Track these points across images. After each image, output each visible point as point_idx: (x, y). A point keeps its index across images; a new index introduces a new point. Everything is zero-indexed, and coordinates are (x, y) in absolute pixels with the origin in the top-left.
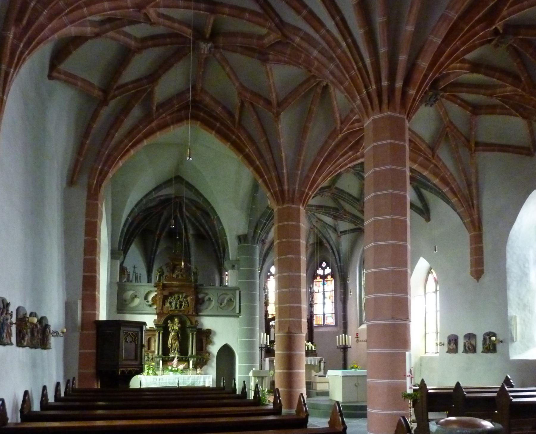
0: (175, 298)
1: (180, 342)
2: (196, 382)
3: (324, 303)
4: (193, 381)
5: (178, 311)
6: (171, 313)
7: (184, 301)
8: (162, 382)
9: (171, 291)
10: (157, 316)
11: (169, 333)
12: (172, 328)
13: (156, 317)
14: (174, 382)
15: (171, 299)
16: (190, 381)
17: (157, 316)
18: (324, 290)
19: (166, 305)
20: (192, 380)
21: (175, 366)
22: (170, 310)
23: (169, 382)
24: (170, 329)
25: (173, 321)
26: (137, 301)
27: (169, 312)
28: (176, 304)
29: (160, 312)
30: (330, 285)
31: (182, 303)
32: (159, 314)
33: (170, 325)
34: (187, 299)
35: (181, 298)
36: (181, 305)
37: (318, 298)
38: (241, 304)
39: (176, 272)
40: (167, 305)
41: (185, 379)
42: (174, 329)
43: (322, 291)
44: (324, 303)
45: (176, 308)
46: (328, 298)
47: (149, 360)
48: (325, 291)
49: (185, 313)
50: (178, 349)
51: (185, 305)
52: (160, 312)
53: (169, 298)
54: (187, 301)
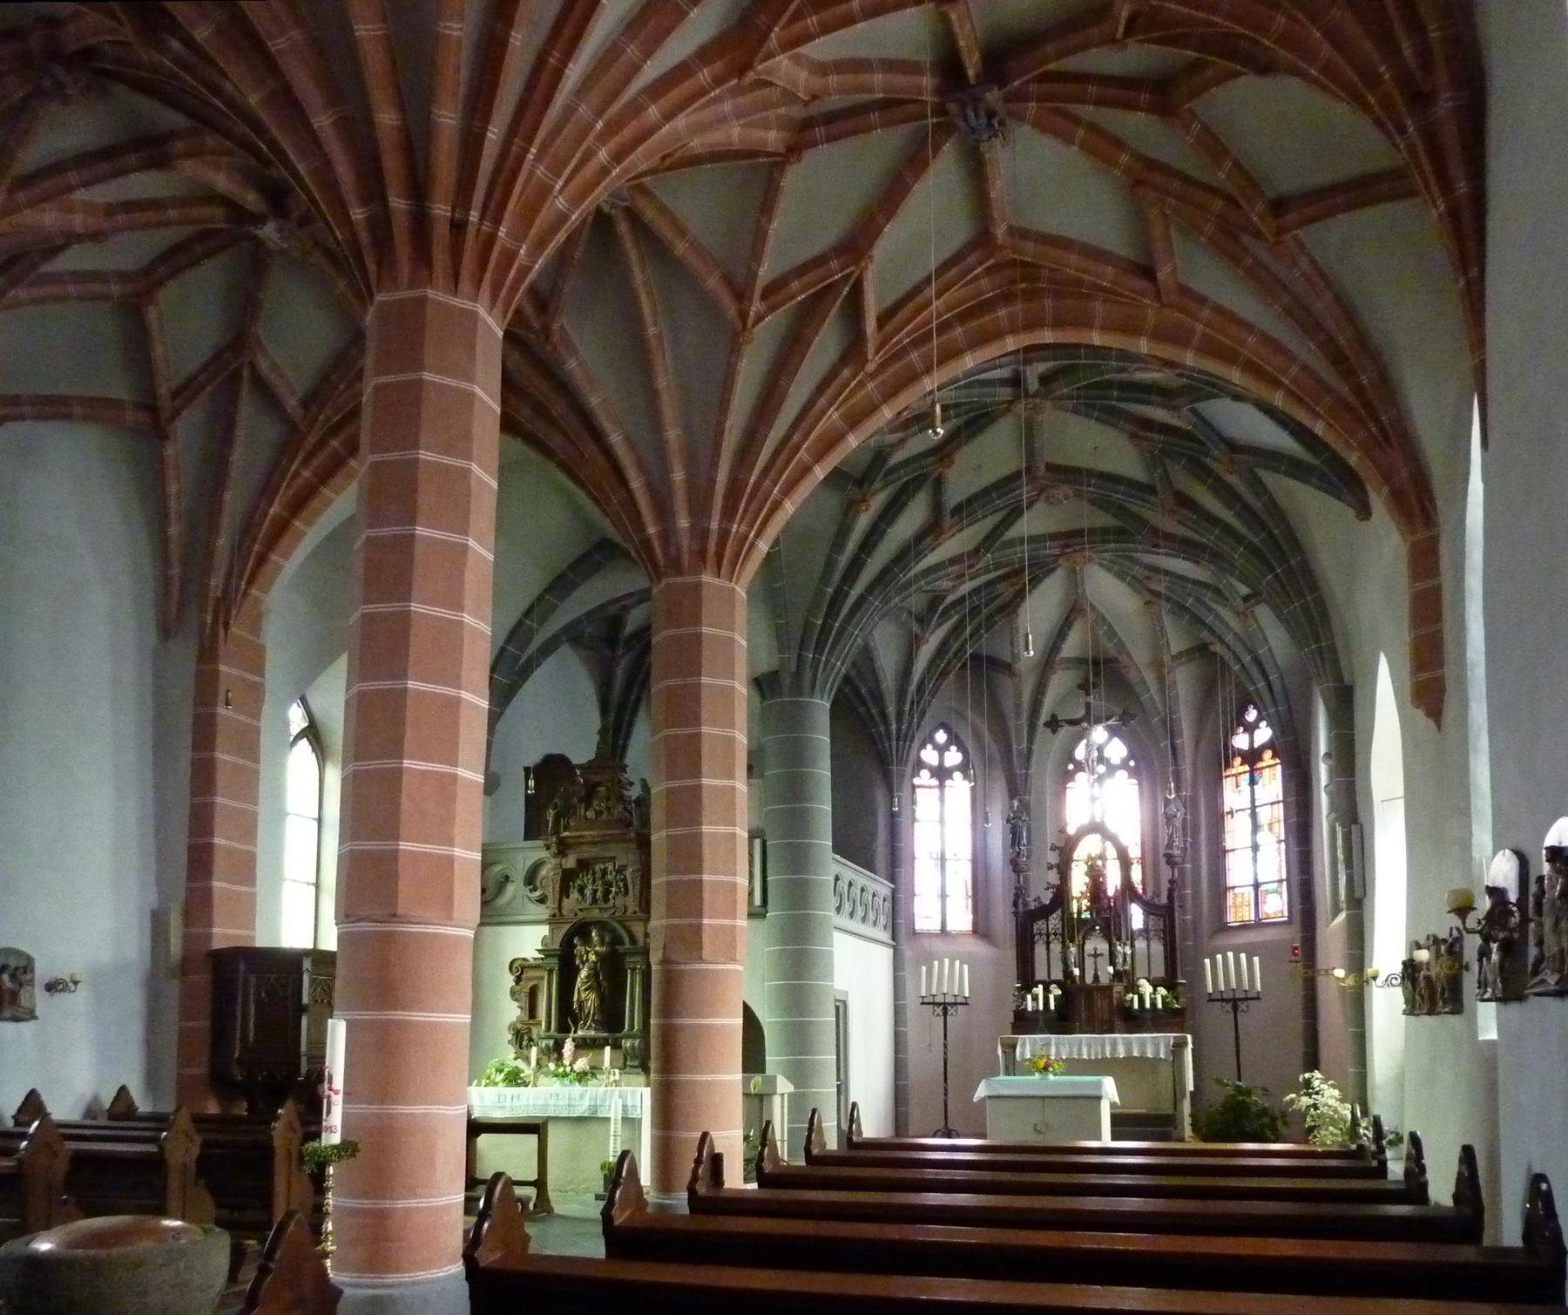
0: (594, 873)
1: (602, 998)
2: (601, 1106)
3: (1255, 848)
4: (593, 1103)
5: (600, 909)
6: (581, 915)
8: (519, 1104)
9: (586, 855)
10: (547, 927)
11: (577, 971)
12: (581, 957)
13: (544, 930)
14: (548, 1105)
16: (586, 1103)
17: (547, 927)
18: (1253, 800)
19: (571, 896)
20: (590, 1099)
21: (566, 1062)
22: (580, 910)
23: (534, 1105)
24: (577, 962)
25: (587, 940)
26: (510, 889)
28: (595, 891)
30: (1272, 783)
32: (554, 921)
33: (580, 949)
34: (625, 876)
36: (607, 893)
37: (1236, 832)
38: (769, 879)
39: (595, 802)
40: (575, 895)
41: (573, 1097)
42: (587, 960)
43: (1249, 805)
44: (1255, 848)
45: (595, 901)
46: (1266, 827)
48: (1257, 803)
49: (617, 914)
50: (594, 1015)
51: (616, 893)
52: (554, 916)
54: (625, 880)
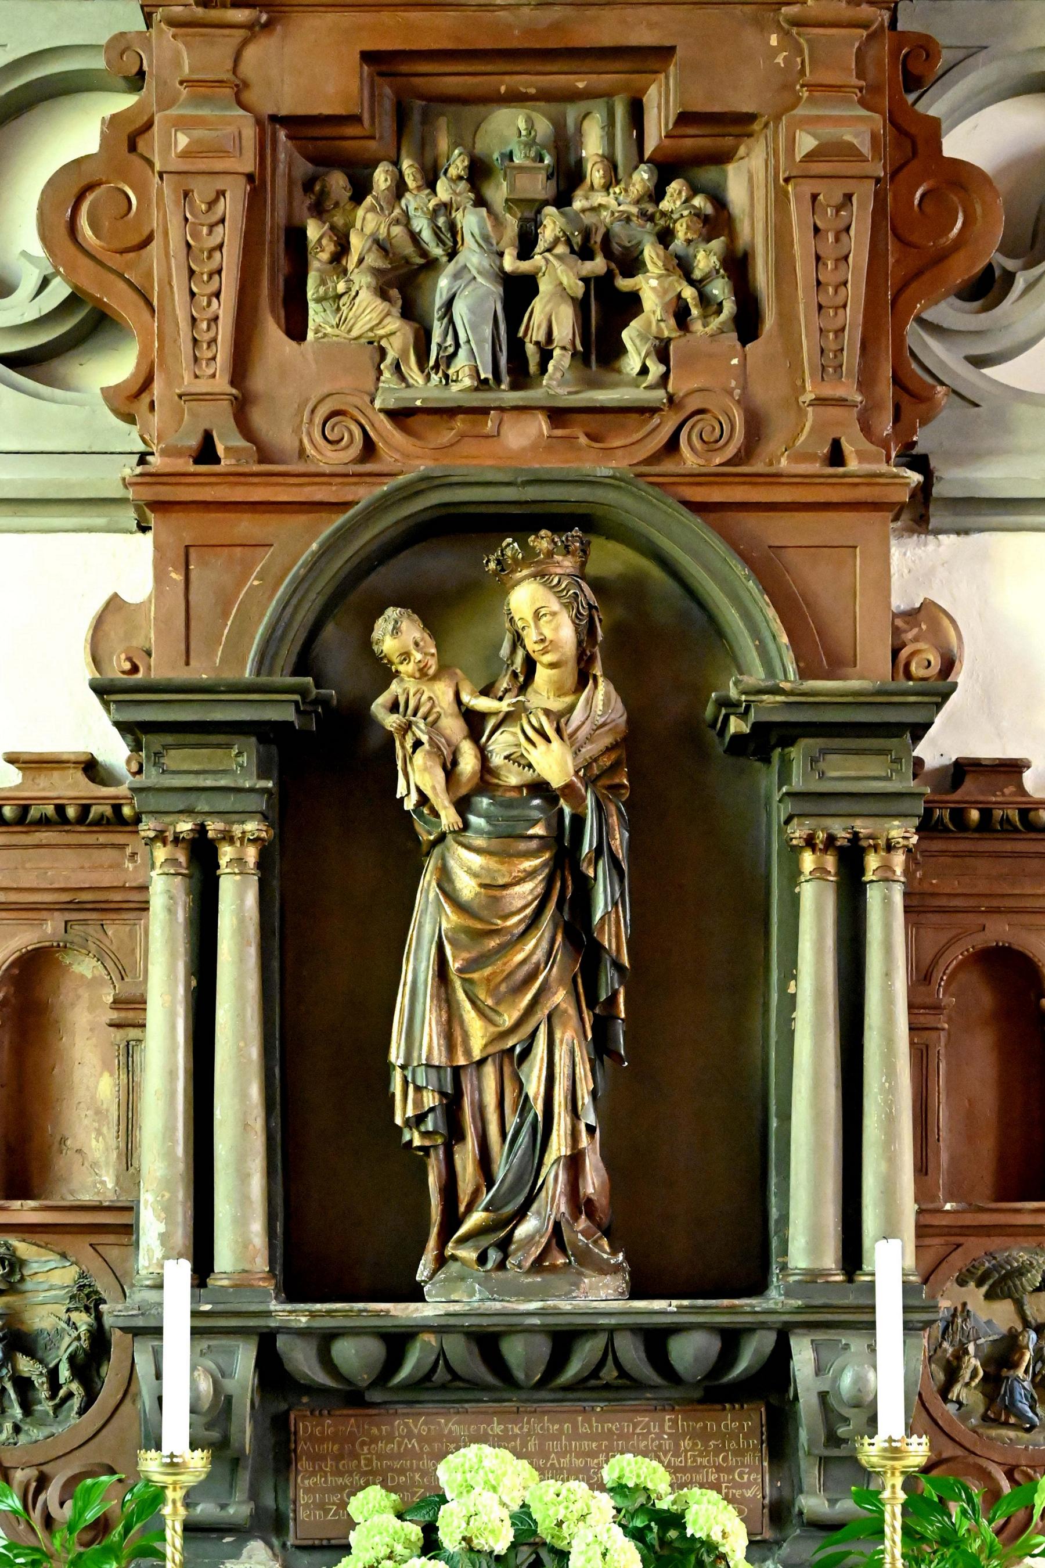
7: (665, 237)
15: (411, 202)
22: (400, 416)
27: (369, 449)
29: (206, 453)
31: (632, 264)
34: (719, 202)
35: (595, 175)
47: (24, 1385)
49: (690, 459)
51: (681, 314)
52: (206, 453)
53: (381, 178)
